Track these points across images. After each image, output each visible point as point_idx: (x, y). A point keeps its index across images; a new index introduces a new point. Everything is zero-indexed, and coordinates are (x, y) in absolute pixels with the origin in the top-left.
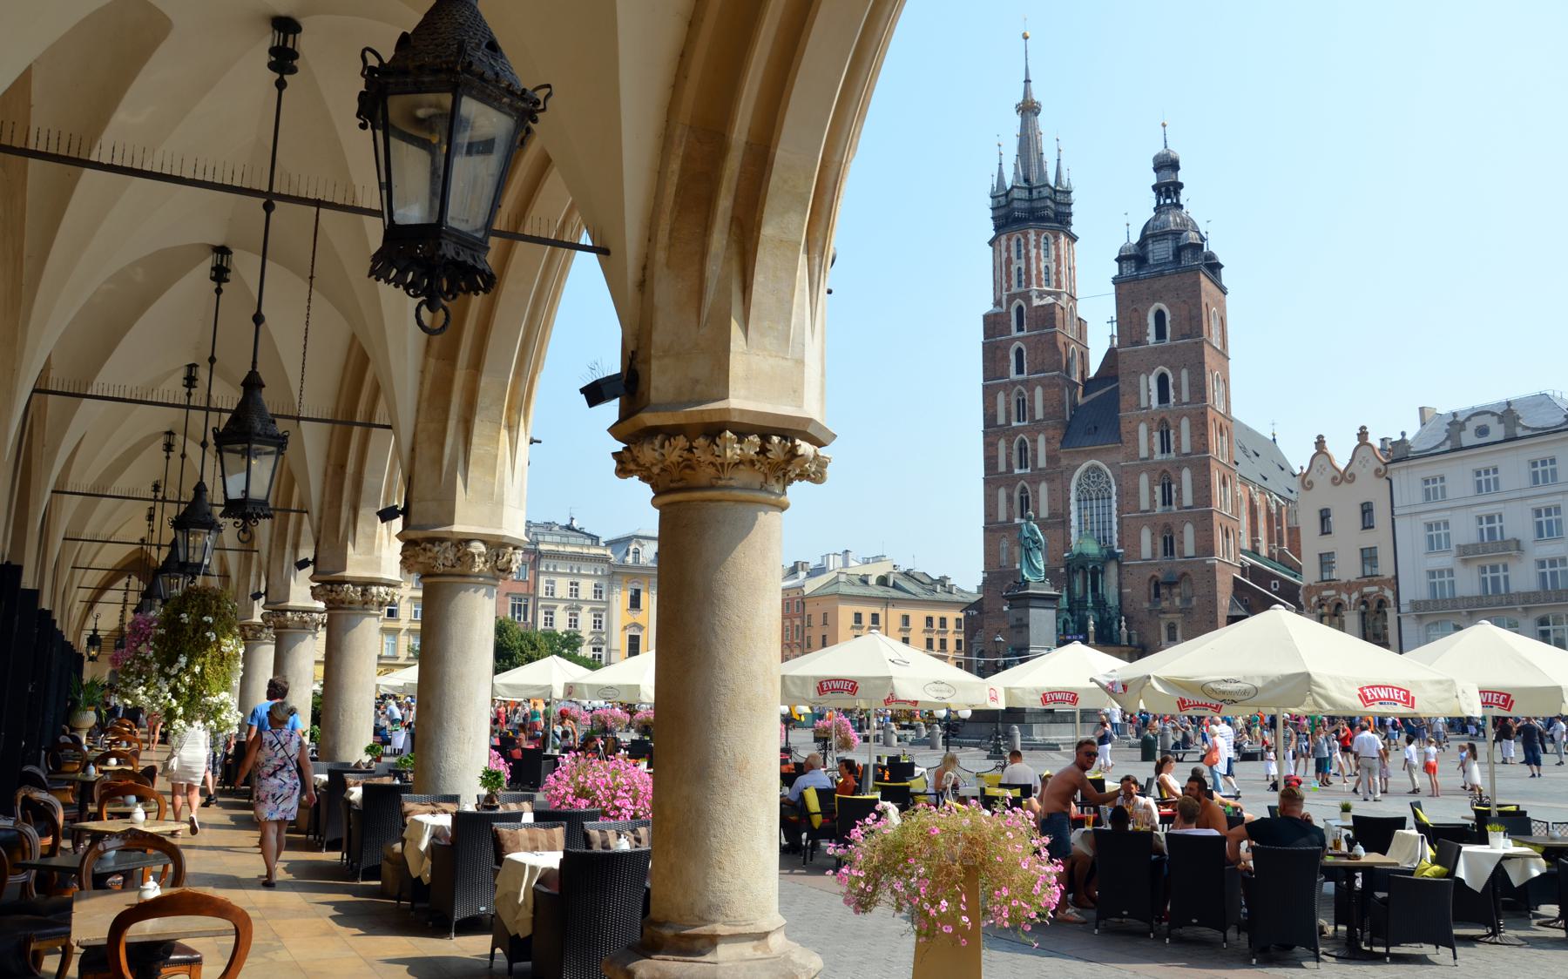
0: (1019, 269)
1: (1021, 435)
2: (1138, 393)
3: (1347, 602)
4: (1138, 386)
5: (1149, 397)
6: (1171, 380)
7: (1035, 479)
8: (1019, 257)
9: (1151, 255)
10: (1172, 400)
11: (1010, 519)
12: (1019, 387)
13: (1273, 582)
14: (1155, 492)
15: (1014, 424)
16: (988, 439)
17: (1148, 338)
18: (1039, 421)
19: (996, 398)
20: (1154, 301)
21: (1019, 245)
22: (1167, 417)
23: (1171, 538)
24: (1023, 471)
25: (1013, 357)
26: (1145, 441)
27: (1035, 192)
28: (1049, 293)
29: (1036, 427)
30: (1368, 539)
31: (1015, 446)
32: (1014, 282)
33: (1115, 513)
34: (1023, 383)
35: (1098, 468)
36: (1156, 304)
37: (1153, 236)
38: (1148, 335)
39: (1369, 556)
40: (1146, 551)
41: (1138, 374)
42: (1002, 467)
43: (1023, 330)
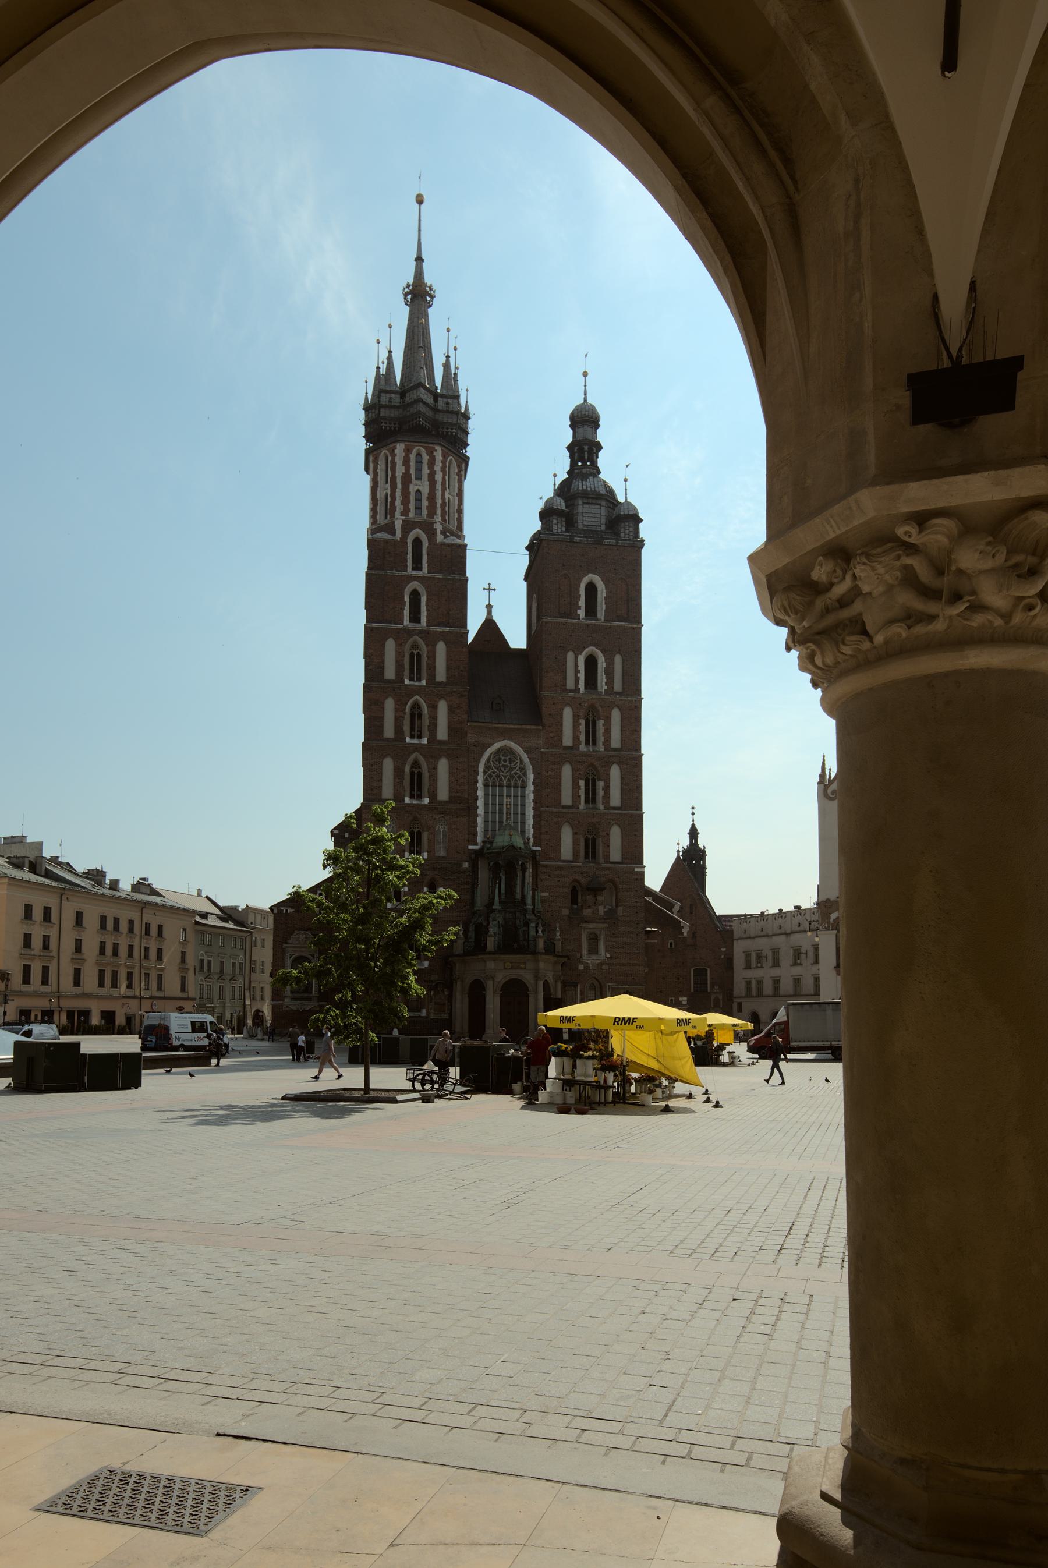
2: (564, 672)
4: (565, 665)
5: (577, 679)
7: (435, 751)
9: (580, 518)
12: (416, 637)
15: (407, 682)
17: (579, 612)
18: (441, 683)
19: (383, 646)
20: (589, 572)
21: (419, 462)
23: (594, 840)
24: (415, 741)
25: (407, 599)
32: (412, 506)
34: (424, 634)
35: (510, 751)
36: (590, 575)
38: (580, 608)
42: (389, 732)
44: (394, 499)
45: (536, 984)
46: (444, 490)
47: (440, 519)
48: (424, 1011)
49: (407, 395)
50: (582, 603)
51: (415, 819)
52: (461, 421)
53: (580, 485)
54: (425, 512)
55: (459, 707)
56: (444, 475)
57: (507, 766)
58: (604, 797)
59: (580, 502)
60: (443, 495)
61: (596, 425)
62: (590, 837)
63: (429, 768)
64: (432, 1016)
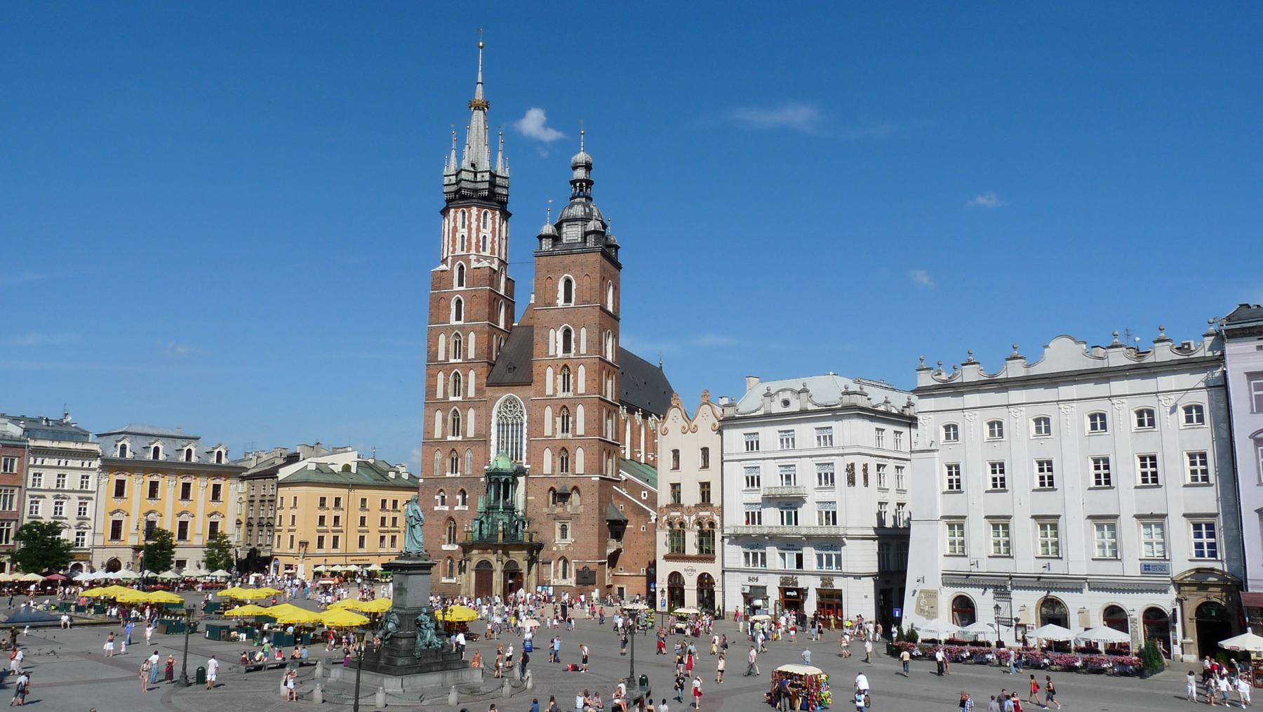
0: (463, 236)
2: (548, 344)
3: (688, 522)
5: (556, 347)
6: (573, 336)
7: (467, 403)
8: (463, 227)
9: (564, 236)
10: (573, 351)
12: (457, 331)
13: (643, 492)
14: (556, 422)
15: (452, 360)
17: (558, 301)
20: (564, 273)
21: (464, 218)
23: (567, 459)
25: (453, 307)
26: (551, 381)
27: (479, 176)
28: (485, 258)
29: (468, 364)
30: (705, 476)
31: (451, 378)
32: (458, 246)
33: (525, 436)
35: (515, 399)
36: (566, 275)
37: (568, 220)
38: (558, 299)
39: (705, 487)
40: (547, 469)
43: (463, 286)
50: (561, 294)
51: (453, 450)
55: (481, 374)
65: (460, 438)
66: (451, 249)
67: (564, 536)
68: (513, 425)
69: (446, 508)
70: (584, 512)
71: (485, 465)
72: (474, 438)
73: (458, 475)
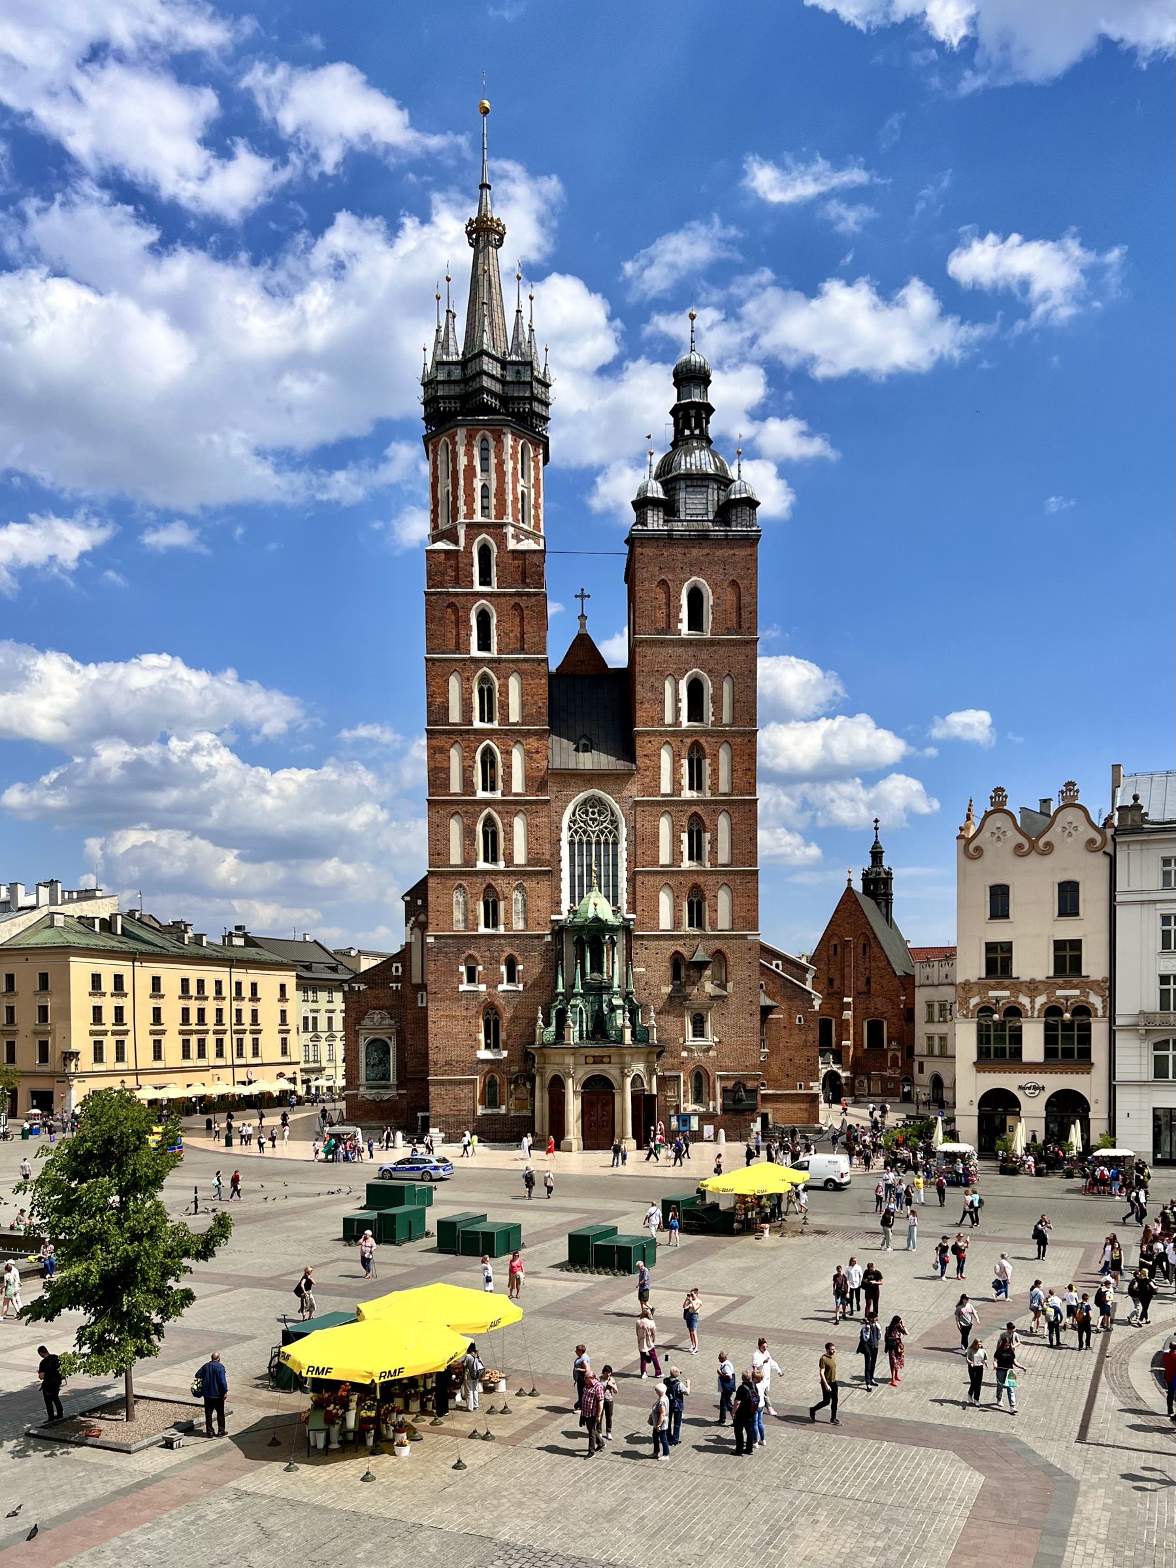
1: (488, 742)
2: (662, 702)
4: (663, 693)
5: (677, 711)
6: (709, 689)
7: (511, 806)
11: (469, 860)
12: (485, 669)
15: (477, 724)
16: (434, 742)
17: (680, 626)
19: (447, 681)
20: (692, 575)
22: (702, 741)
25: (474, 622)
35: (600, 802)
36: (694, 578)
38: (681, 621)
41: (662, 675)
42: (456, 786)
44: (456, 498)
45: (623, 1081)
46: (515, 481)
47: (510, 520)
48: (504, 1107)
49: (469, 365)
50: (684, 614)
51: (490, 886)
52: (538, 389)
53: (683, 462)
54: (493, 512)
55: (537, 752)
56: (515, 463)
57: (596, 819)
58: (710, 852)
59: (683, 485)
60: (514, 489)
61: (707, 382)
62: (695, 900)
63: (504, 825)
64: (512, 1114)
65: (501, 865)
66: (463, 509)
67: (699, 1031)
68: (598, 843)
69: (482, 988)
70: (735, 993)
71: (553, 913)
72: (525, 866)
73: (502, 930)
